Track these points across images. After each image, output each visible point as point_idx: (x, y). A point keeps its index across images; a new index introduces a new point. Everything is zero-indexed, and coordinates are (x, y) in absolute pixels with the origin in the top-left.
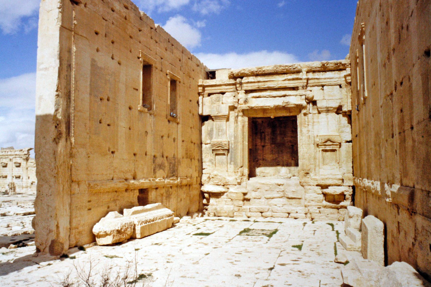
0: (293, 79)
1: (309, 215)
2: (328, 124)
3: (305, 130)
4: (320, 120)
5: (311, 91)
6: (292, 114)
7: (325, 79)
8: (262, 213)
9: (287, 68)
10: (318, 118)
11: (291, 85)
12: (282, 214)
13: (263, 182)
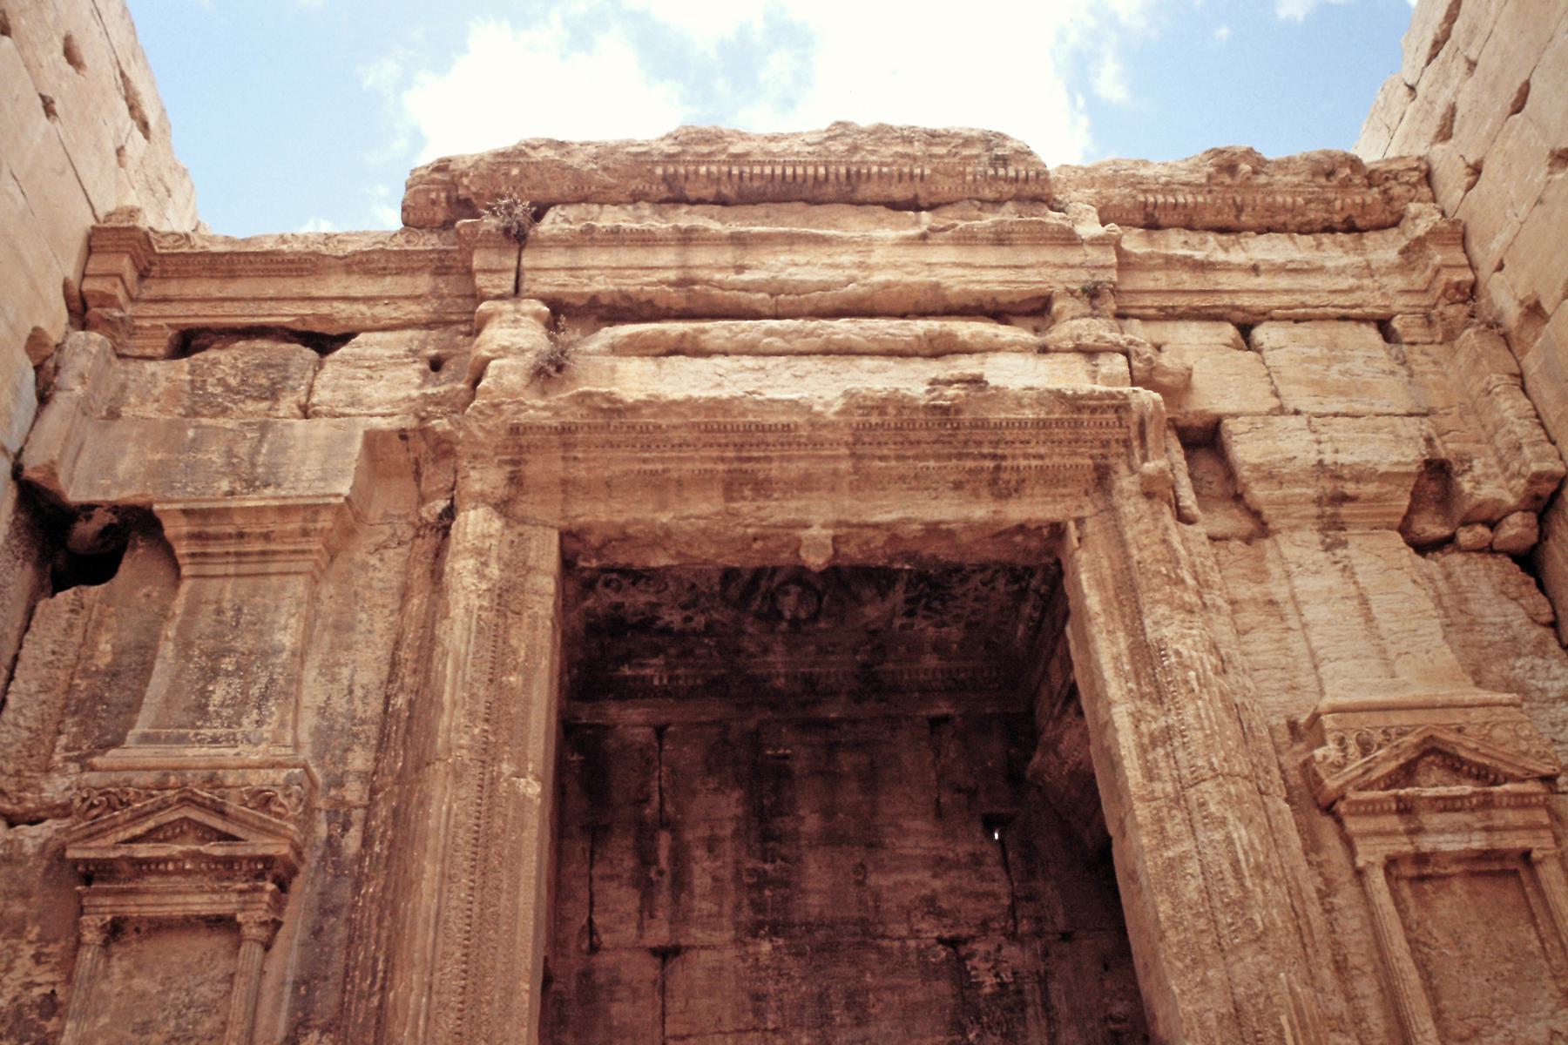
2: (1369, 618)
4: (1281, 592)
6: (1017, 511)
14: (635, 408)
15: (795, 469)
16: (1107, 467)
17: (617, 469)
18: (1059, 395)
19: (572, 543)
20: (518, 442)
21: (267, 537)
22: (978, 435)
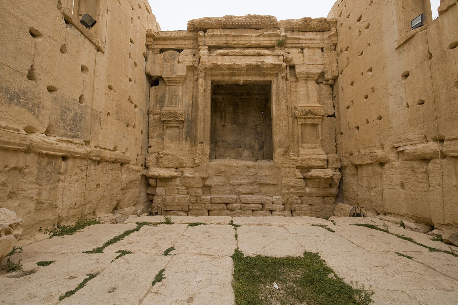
0: (269, 36)
1: (288, 206)
3: (282, 98)
5: (289, 53)
6: (266, 79)
7: (306, 39)
8: (227, 204)
9: (263, 20)
10: (296, 87)
11: (267, 42)
12: (254, 205)
13: (229, 164)
14: (219, 66)
15: (239, 73)
16: (278, 74)
17: (217, 73)
18: (273, 64)
19: (212, 82)
20: (205, 70)
21: (176, 80)
22: (262, 69)
